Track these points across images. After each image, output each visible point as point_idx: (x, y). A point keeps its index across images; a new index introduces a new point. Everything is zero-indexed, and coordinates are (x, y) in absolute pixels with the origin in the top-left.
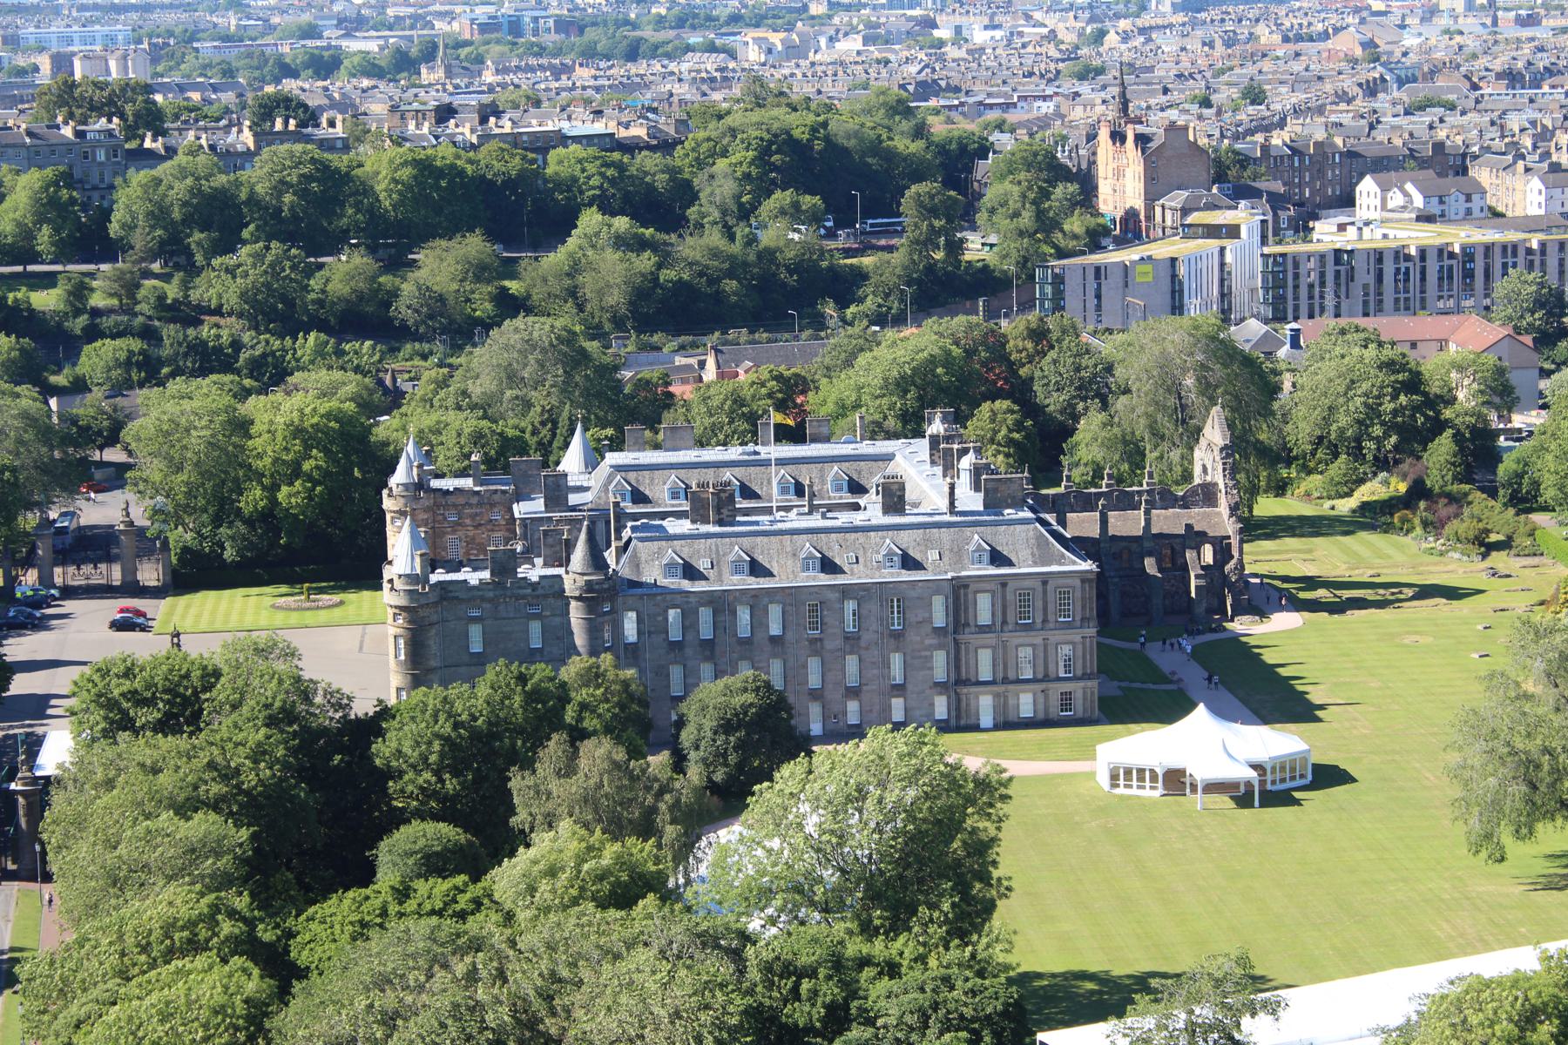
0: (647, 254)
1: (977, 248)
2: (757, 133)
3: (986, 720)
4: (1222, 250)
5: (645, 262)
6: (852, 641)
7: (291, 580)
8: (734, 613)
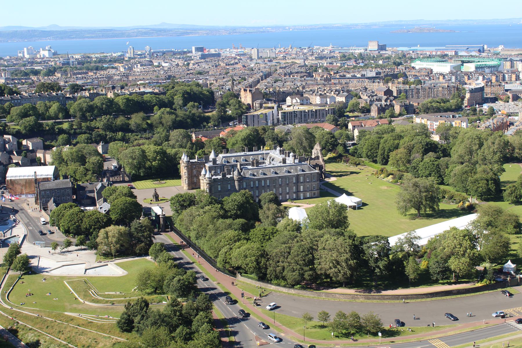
3: (302, 198)
5: (173, 117)
6: (280, 186)
7: (152, 179)
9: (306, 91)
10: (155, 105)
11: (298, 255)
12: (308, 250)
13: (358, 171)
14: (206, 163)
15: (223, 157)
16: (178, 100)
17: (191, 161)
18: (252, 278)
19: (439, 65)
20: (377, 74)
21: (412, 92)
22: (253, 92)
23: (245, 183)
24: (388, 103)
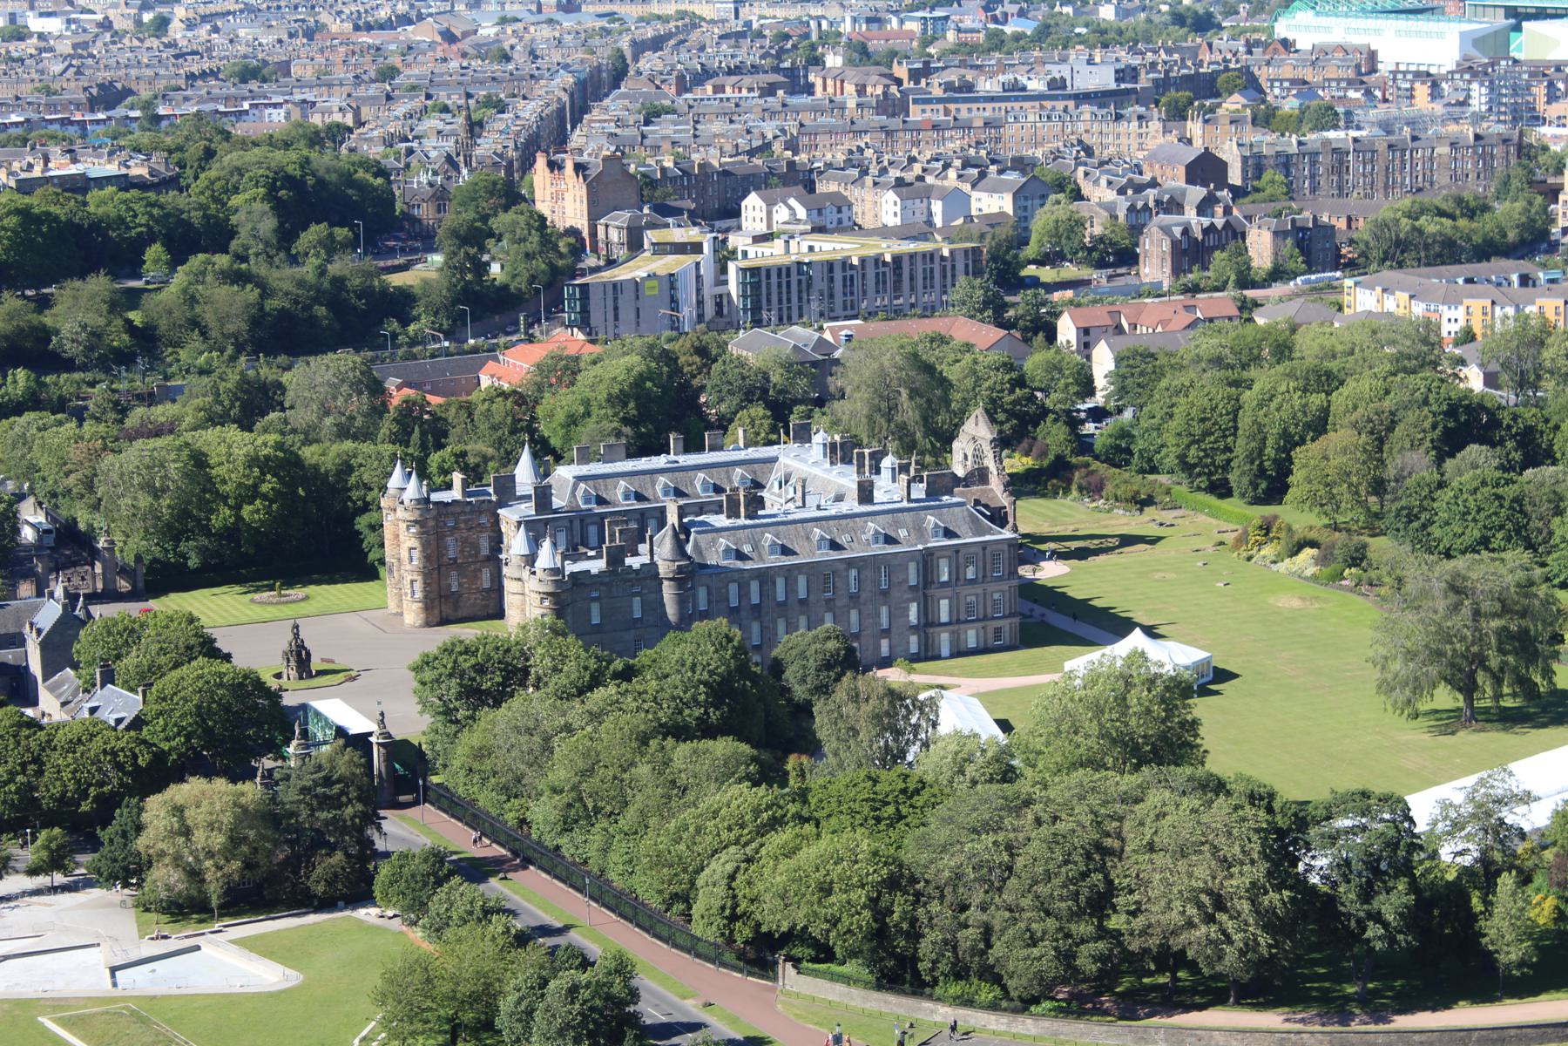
0: (249, 287)
2: (261, 172)
3: (945, 651)
4: (698, 264)
5: (251, 294)
6: (854, 599)
8: (774, 583)
9: (829, 165)
10: (149, 238)
11: (1048, 876)
12: (1088, 856)
13: (1152, 530)
14: (502, 504)
15: (579, 479)
16: (252, 216)
17: (435, 497)
18: (847, 980)
19: (1407, 33)
20: (1121, 75)
21: (1313, 163)
22: (593, 173)
23: (702, 593)
24: (1219, 222)
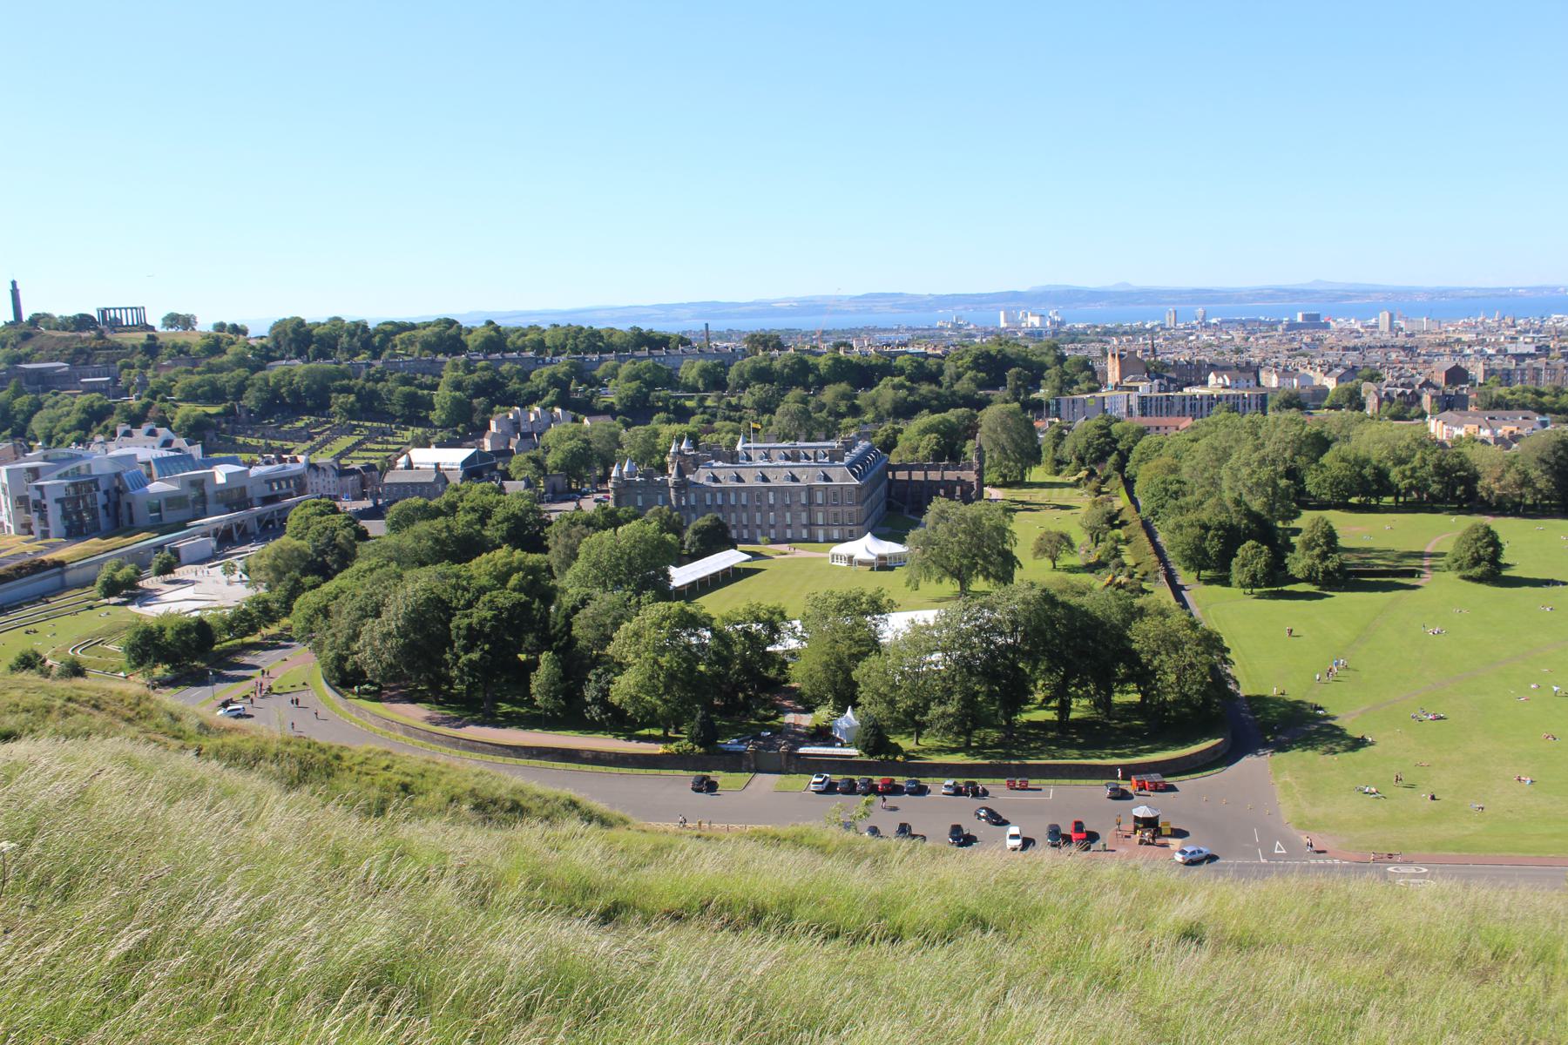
1: (1042, 394)
3: (821, 538)
5: (902, 393)
6: (771, 507)
21: (1523, 374)
